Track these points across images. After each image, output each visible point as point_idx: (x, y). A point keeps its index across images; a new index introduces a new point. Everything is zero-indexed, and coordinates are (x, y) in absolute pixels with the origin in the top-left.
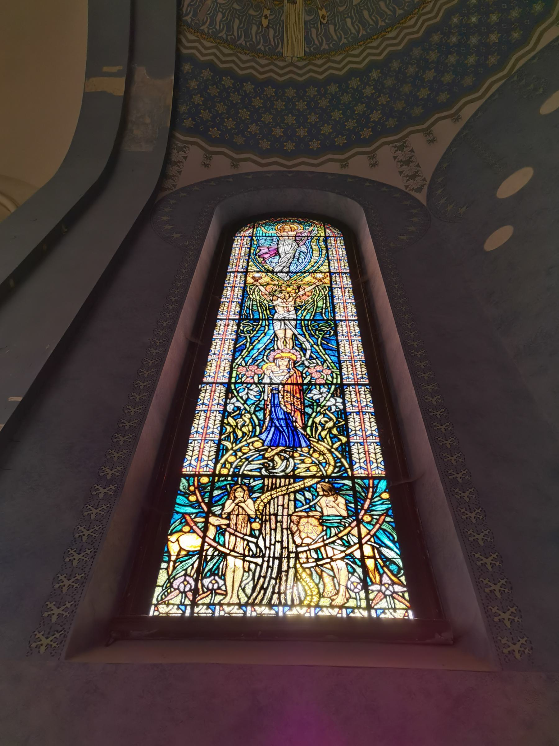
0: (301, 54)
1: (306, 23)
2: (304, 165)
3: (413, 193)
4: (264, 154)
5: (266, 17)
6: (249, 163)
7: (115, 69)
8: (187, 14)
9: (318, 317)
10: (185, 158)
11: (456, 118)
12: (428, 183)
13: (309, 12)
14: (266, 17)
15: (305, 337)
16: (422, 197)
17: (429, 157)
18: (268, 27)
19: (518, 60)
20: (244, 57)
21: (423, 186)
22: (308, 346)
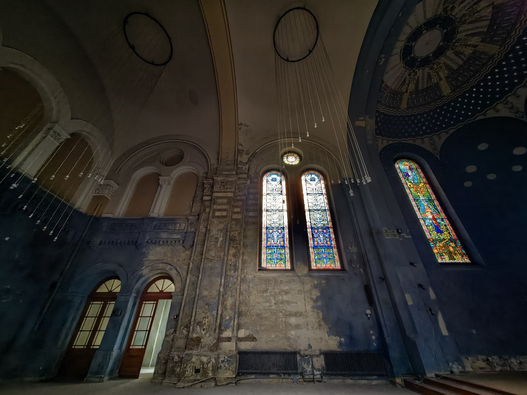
11: (447, 133)
16: (438, 157)
17: (439, 143)
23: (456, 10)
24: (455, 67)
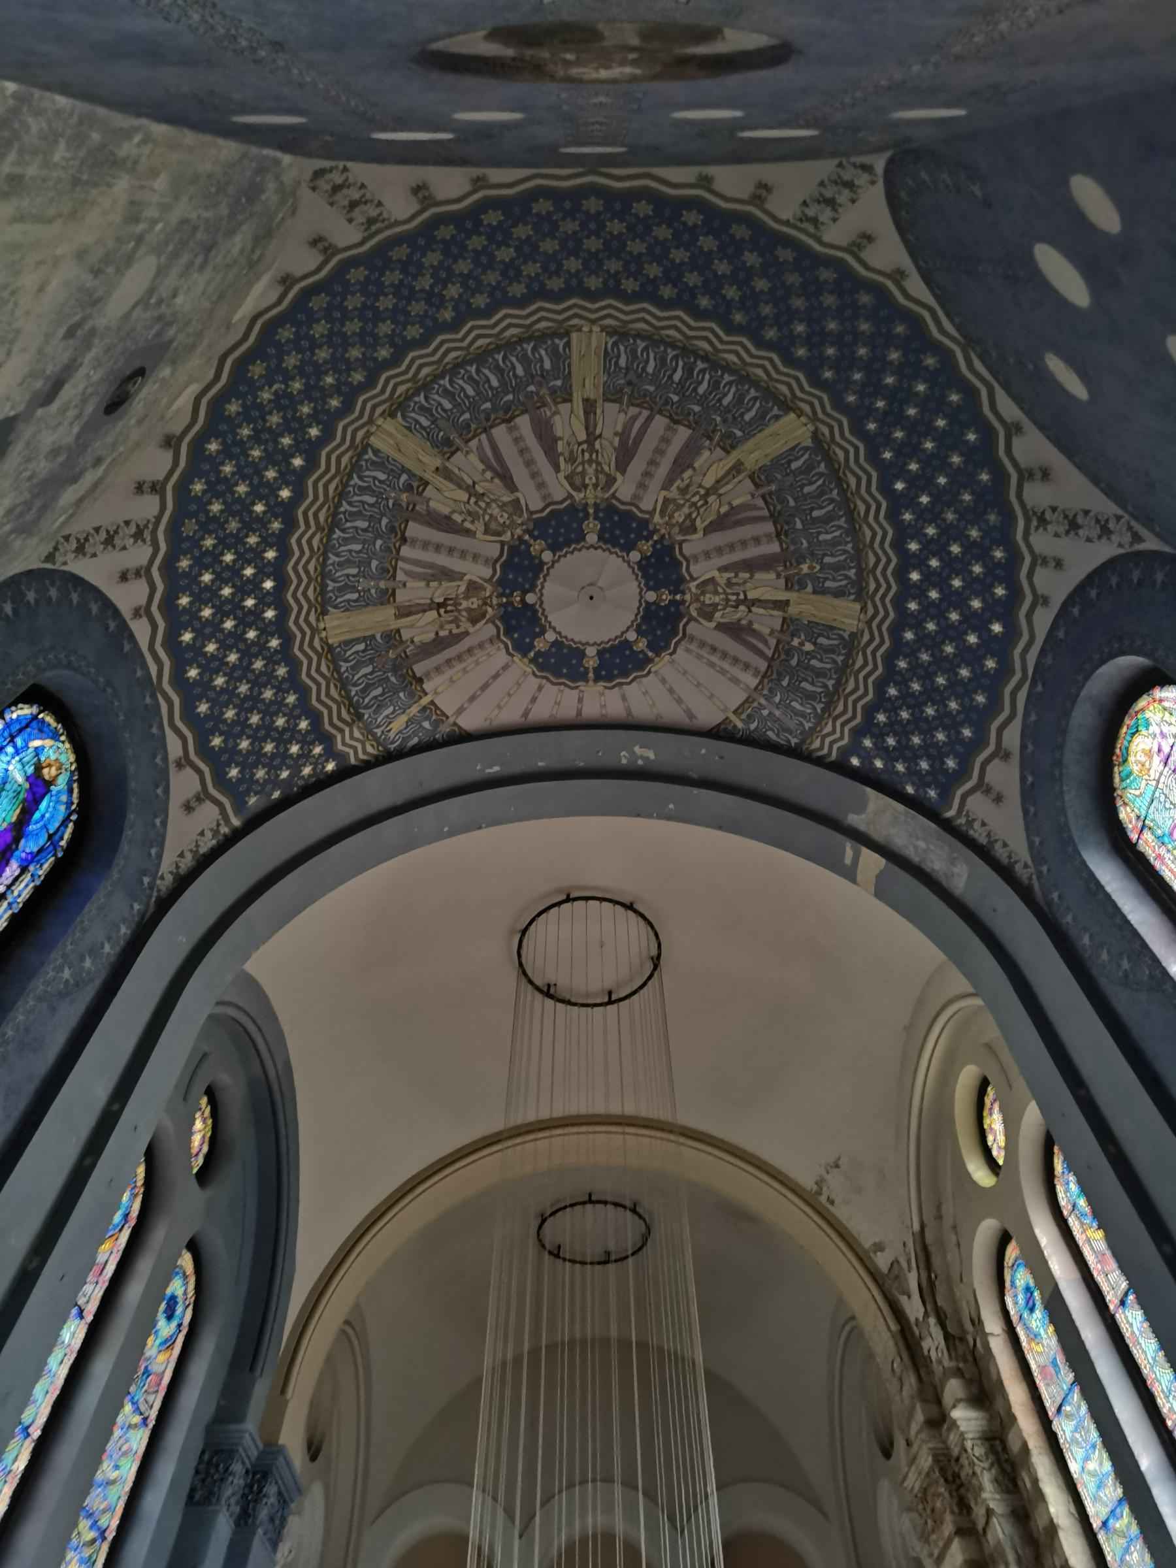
0: (858, 606)
1: (815, 592)
2: (1027, 656)
5: (802, 644)
6: (1006, 733)
8: (789, 741)
10: (984, 824)
12: (1126, 517)
13: (802, 586)
14: (802, 644)
17: (1072, 488)
18: (815, 644)
19: (943, 330)
20: (851, 686)
21: (1130, 528)
23: (479, 572)
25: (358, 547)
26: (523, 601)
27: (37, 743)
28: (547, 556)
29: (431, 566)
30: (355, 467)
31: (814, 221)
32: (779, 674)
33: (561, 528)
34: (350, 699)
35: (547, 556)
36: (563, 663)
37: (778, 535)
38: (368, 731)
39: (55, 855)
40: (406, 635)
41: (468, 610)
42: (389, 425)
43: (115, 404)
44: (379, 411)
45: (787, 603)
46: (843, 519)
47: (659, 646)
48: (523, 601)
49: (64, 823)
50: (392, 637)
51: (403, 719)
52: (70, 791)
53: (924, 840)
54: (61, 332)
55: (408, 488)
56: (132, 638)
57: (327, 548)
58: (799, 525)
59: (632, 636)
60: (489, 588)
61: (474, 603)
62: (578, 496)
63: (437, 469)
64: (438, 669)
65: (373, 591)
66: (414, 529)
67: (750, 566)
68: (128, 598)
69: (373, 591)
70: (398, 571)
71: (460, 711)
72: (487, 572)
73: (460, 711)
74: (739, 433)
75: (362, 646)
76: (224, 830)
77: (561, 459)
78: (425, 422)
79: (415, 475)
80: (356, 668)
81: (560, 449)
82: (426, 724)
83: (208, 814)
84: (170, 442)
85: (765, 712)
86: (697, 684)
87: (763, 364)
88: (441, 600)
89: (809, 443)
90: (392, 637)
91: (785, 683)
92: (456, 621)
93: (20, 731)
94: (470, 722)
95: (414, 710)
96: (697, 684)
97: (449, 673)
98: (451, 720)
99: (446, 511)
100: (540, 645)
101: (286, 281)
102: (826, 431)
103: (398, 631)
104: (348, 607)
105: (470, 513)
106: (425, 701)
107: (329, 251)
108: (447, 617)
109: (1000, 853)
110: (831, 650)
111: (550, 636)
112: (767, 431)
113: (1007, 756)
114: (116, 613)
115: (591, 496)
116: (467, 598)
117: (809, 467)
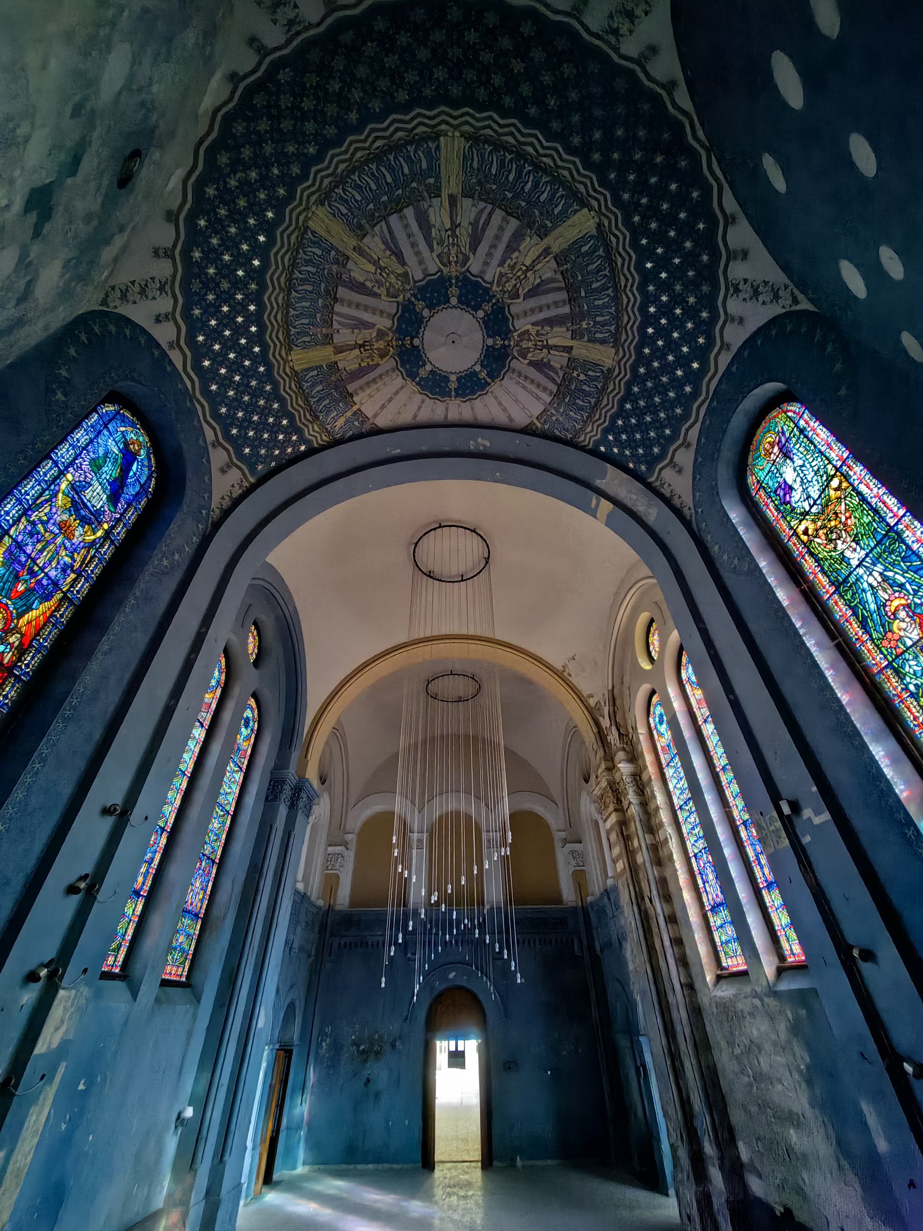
0: (613, 351)
1: (589, 341)
2: (710, 384)
3: (794, 308)
4: (686, 416)
5: (578, 375)
7: (594, 502)
9: (879, 538)
11: (730, 220)
12: (791, 286)
15: (891, 571)
16: (805, 305)
18: (586, 375)
19: (696, 136)
21: (792, 294)
22: (903, 580)
23: (384, 323)
24: (514, 223)
25: (307, 304)
26: (412, 343)
27: (123, 429)
28: (426, 313)
29: (354, 318)
30: (300, 245)
31: (615, 32)
32: (564, 394)
33: (434, 293)
34: (310, 406)
35: (426, 313)
36: (436, 385)
37: (570, 300)
38: (322, 426)
39: (147, 497)
40: (341, 365)
41: (377, 349)
42: (321, 212)
43: (125, 180)
44: (313, 198)
45: (571, 348)
46: (611, 290)
47: (493, 375)
48: (412, 343)
49: (149, 478)
50: (333, 366)
51: (342, 420)
52: (149, 459)
53: (637, 495)
54: (68, 110)
55: (337, 262)
56: (171, 363)
57: (288, 304)
58: (583, 294)
59: (478, 368)
60: (391, 334)
61: (381, 344)
62: (445, 270)
63: (354, 248)
64: (361, 388)
65: (319, 336)
66: (342, 292)
67: (551, 322)
68: (164, 334)
69: (319, 336)
70: (334, 322)
71: (375, 416)
72: (389, 323)
73: (375, 416)
74: (550, 225)
75: (315, 373)
76: (246, 484)
77: (435, 243)
78: (345, 211)
79: (340, 252)
80: (313, 386)
81: (433, 234)
82: (356, 423)
83: (234, 475)
84: (171, 217)
85: (554, 418)
86: (516, 400)
87: (570, 166)
88: (361, 342)
89: (594, 232)
90: (333, 366)
91: (567, 400)
92: (371, 357)
93: (110, 421)
94: (382, 421)
95: (349, 414)
96: (516, 400)
97: (368, 391)
98: (371, 421)
99: (361, 279)
100: (423, 373)
101: (234, 78)
102: (606, 224)
103: (336, 363)
104: (305, 346)
105: (377, 281)
106: (355, 408)
107: (263, 51)
108: (365, 354)
109: (676, 502)
110: (596, 379)
111: (428, 367)
112: (570, 222)
113: (689, 445)
114: (158, 345)
115: (453, 271)
116: (377, 341)
117: (594, 250)
